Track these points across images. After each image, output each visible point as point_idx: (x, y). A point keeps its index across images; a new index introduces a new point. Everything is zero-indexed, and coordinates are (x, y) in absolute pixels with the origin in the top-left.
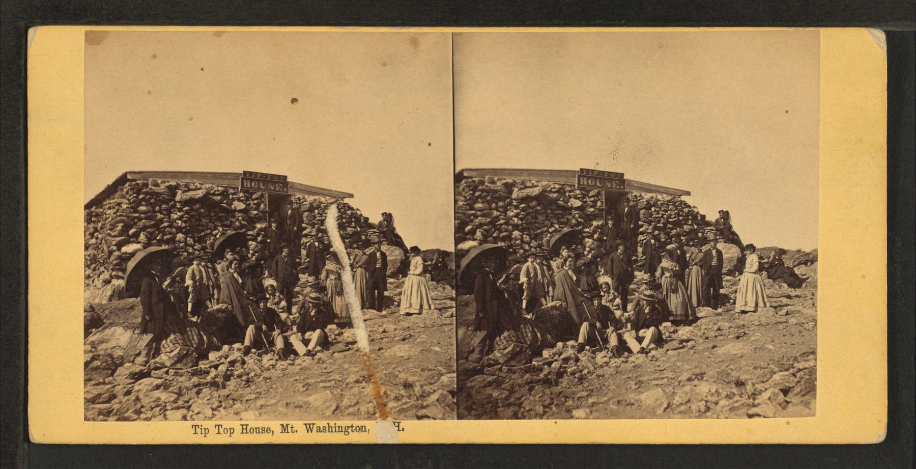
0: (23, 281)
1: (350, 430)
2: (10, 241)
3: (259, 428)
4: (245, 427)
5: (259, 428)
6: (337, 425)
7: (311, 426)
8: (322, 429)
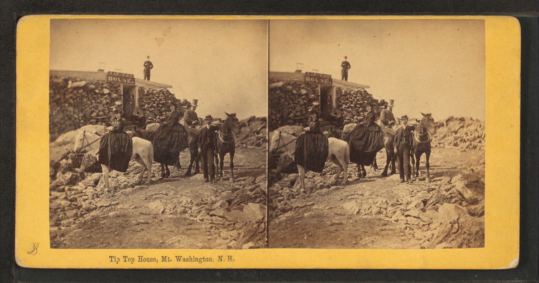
1: (202, 260)
3: (149, 259)
4: (140, 258)
5: (149, 259)
6: (195, 258)
7: (180, 257)
8: (186, 259)
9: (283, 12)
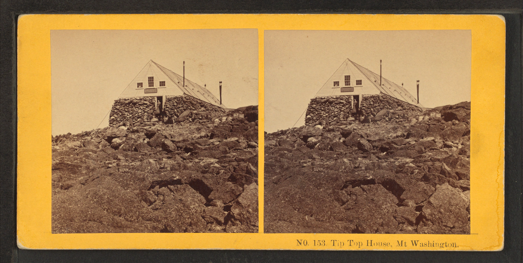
0: (14, 160)
2: (7, 136)
9: (273, 10)
